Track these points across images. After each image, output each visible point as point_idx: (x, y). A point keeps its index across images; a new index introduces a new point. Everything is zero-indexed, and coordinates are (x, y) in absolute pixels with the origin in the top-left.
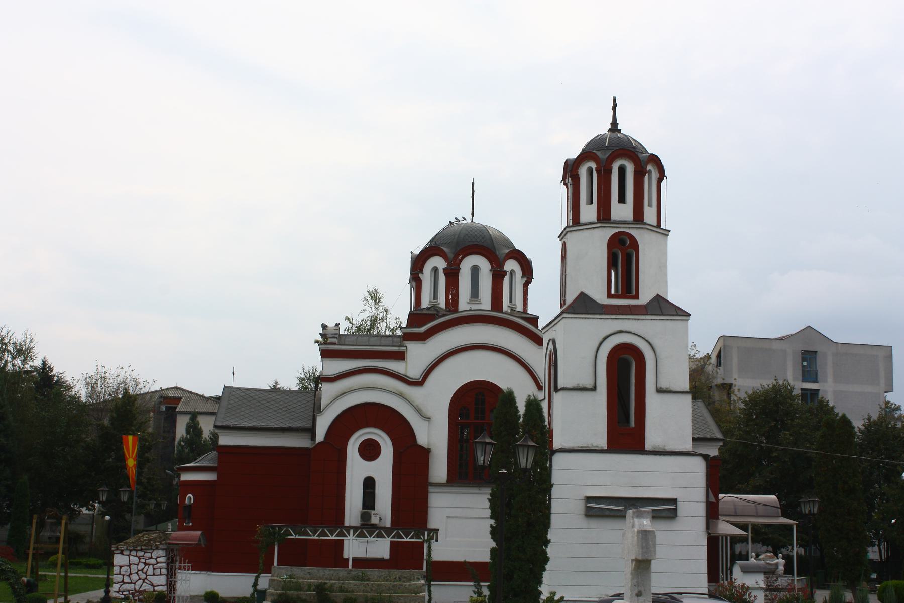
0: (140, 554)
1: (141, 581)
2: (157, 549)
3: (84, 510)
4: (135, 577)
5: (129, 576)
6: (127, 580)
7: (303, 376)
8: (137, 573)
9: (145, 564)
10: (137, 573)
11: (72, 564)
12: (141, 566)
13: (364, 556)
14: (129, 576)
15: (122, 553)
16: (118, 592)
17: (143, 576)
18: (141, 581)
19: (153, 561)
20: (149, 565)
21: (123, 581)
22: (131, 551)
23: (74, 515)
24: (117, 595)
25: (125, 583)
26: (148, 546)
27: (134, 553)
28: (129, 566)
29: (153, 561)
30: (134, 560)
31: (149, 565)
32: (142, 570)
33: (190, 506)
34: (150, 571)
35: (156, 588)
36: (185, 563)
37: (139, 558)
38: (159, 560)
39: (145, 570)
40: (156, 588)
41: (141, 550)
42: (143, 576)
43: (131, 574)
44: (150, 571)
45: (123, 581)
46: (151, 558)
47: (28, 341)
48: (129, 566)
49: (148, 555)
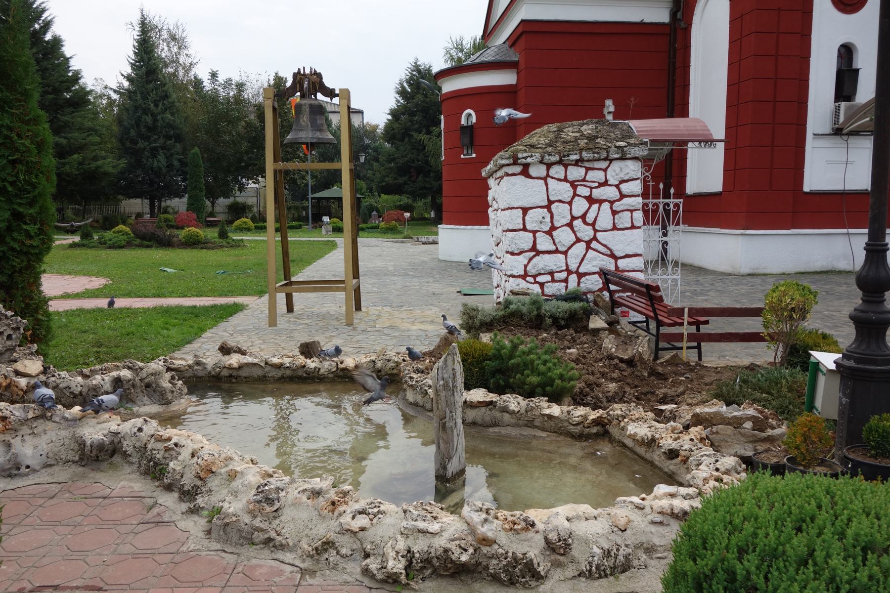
0: (576, 173)
1: (581, 246)
2: (623, 158)
3: (251, 185)
4: (564, 236)
5: (549, 233)
6: (544, 243)
7: (451, 46)
8: (570, 225)
9: (591, 200)
10: (570, 225)
11: (256, 228)
12: (580, 206)
13: (837, 186)
14: (549, 233)
15: (525, 173)
16: (524, 277)
17: (586, 233)
18: (583, 245)
19: (610, 192)
20: (600, 202)
21: (534, 248)
22: (549, 166)
23: (242, 188)
24: (522, 285)
25: (539, 253)
26: (596, 153)
27: (558, 171)
28: (548, 207)
29: (610, 192)
30: (562, 190)
31: (600, 202)
32: (583, 217)
33: (470, 129)
34: (605, 219)
35: (622, 263)
36: (667, 196)
37: (574, 185)
38: (625, 188)
39: (590, 218)
40: (622, 263)
41: (577, 163)
42: (586, 233)
43: (553, 228)
44: (605, 219)
45: (534, 248)
46: (605, 183)
47: (180, 30)
48: (548, 207)
49: (596, 176)
